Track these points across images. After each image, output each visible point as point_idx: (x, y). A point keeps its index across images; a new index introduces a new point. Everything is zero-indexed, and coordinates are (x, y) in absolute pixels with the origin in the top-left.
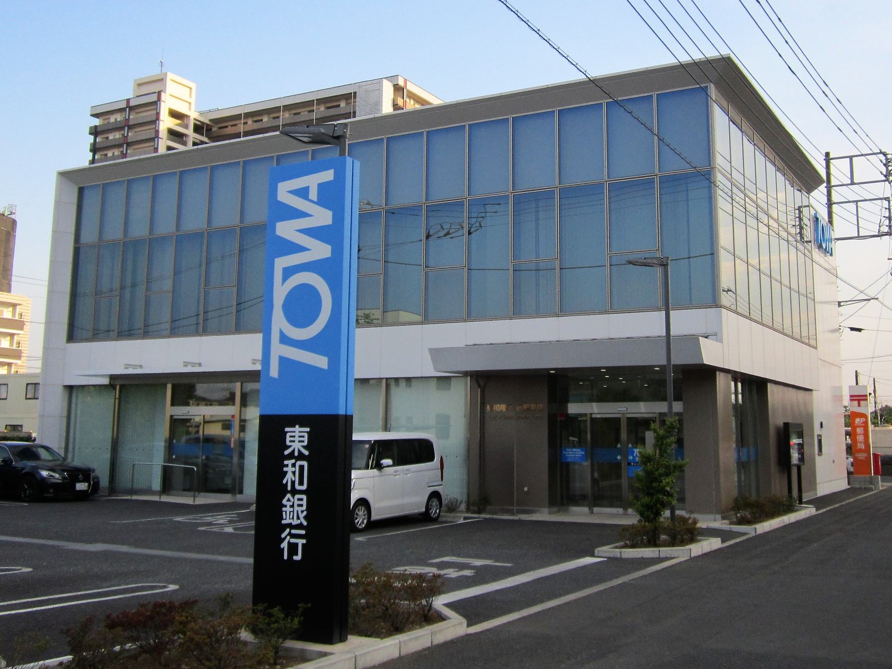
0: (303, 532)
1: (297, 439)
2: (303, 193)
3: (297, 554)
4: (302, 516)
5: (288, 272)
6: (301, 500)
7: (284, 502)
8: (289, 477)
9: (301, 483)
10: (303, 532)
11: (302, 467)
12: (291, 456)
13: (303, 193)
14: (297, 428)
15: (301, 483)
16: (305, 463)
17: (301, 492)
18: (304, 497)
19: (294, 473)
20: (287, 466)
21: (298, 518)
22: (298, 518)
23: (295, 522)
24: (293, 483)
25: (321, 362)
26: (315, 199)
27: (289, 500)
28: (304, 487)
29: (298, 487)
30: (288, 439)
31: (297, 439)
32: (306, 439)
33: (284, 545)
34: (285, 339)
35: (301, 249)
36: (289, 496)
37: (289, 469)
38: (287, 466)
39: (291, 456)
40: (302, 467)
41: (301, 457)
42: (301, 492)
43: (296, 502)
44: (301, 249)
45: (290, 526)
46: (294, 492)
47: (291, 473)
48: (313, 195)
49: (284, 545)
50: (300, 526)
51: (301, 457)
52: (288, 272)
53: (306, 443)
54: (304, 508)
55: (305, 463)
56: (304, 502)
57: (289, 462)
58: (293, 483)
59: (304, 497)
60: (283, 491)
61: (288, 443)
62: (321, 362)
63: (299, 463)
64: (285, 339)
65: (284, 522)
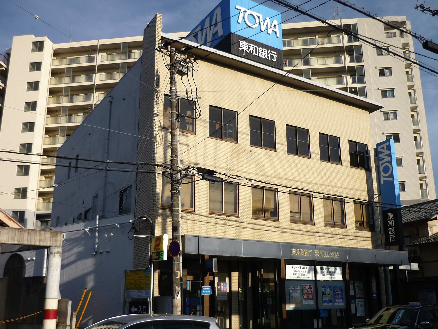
3: (393, 240)
4: (394, 232)
8: (390, 224)
9: (393, 225)
11: (392, 222)
12: (390, 220)
13: (383, 148)
14: (390, 213)
15: (393, 225)
16: (393, 221)
18: (394, 228)
19: (391, 223)
20: (389, 222)
21: (393, 232)
22: (393, 232)
23: (392, 233)
24: (391, 225)
25: (391, 179)
26: (386, 149)
27: (390, 229)
28: (394, 226)
29: (392, 226)
30: (388, 216)
32: (392, 215)
33: (390, 239)
34: (383, 177)
36: (390, 228)
37: (390, 223)
38: (389, 222)
39: (390, 220)
40: (392, 222)
41: (392, 219)
45: (391, 235)
46: (391, 227)
47: (390, 224)
48: (385, 148)
49: (390, 239)
50: (394, 234)
51: (392, 219)
52: (382, 164)
53: (392, 216)
55: (393, 221)
56: (394, 229)
57: (389, 221)
58: (391, 225)
59: (394, 228)
61: (388, 217)
62: (391, 179)
64: (383, 177)
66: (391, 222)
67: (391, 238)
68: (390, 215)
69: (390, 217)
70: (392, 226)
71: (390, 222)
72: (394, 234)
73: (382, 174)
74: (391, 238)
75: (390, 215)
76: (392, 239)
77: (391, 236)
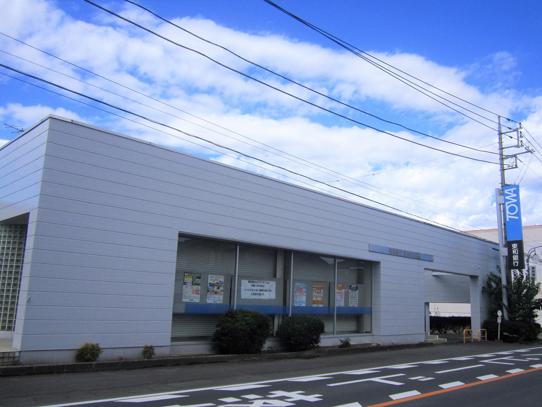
1: (515, 246)
2: (510, 192)
4: (517, 259)
5: (508, 205)
7: (513, 256)
11: (516, 251)
13: (510, 192)
16: (517, 250)
24: (515, 253)
28: (518, 254)
30: (513, 246)
31: (515, 246)
34: (509, 215)
35: (511, 201)
39: (514, 249)
40: (516, 251)
44: (511, 201)
45: (515, 260)
46: (515, 255)
47: (514, 252)
48: (512, 192)
49: (514, 264)
51: (516, 249)
52: (508, 205)
55: (517, 250)
57: (514, 250)
58: (515, 253)
60: (513, 254)
63: (516, 250)
64: (509, 215)
66: (516, 251)
67: (515, 263)
69: (515, 247)
72: (518, 260)
73: (508, 212)
74: (515, 263)
75: (515, 246)
76: (516, 264)
77: (515, 262)
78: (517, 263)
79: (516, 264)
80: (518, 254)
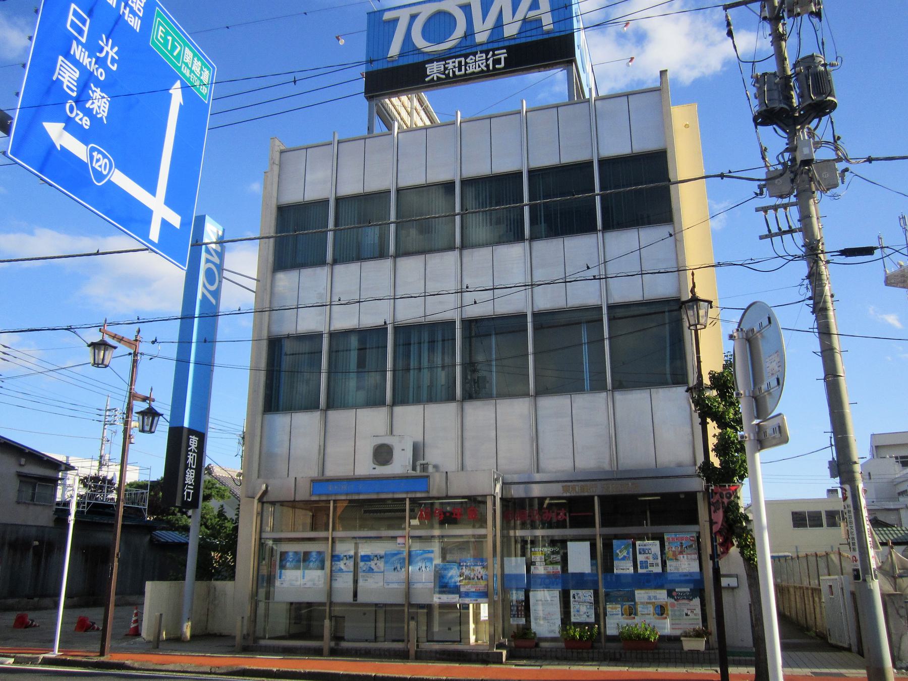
0: (192, 487)
4: (193, 481)
6: (193, 472)
8: (190, 460)
9: (194, 465)
10: (192, 487)
11: (194, 456)
14: (194, 437)
15: (194, 465)
17: (193, 469)
18: (194, 471)
23: (190, 483)
24: (191, 464)
28: (194, 467)
32: (196, 443)
33: (185, 493)
40: (194, 456)
42: (193, 469)
43: (191, 473)
46: (191, 468)
54: (193, 477)
55: (196, 455)
56: (194, 474)
58: (191, 464)
63: (194, 454)
65: (186, 482)
68: (194, 440)
70: (192, 466)
71: (192, 455)
76: (188, 493)
77: (188, 488)
78: (192, 491)
79: (188, 493)
80: (194, 467)
